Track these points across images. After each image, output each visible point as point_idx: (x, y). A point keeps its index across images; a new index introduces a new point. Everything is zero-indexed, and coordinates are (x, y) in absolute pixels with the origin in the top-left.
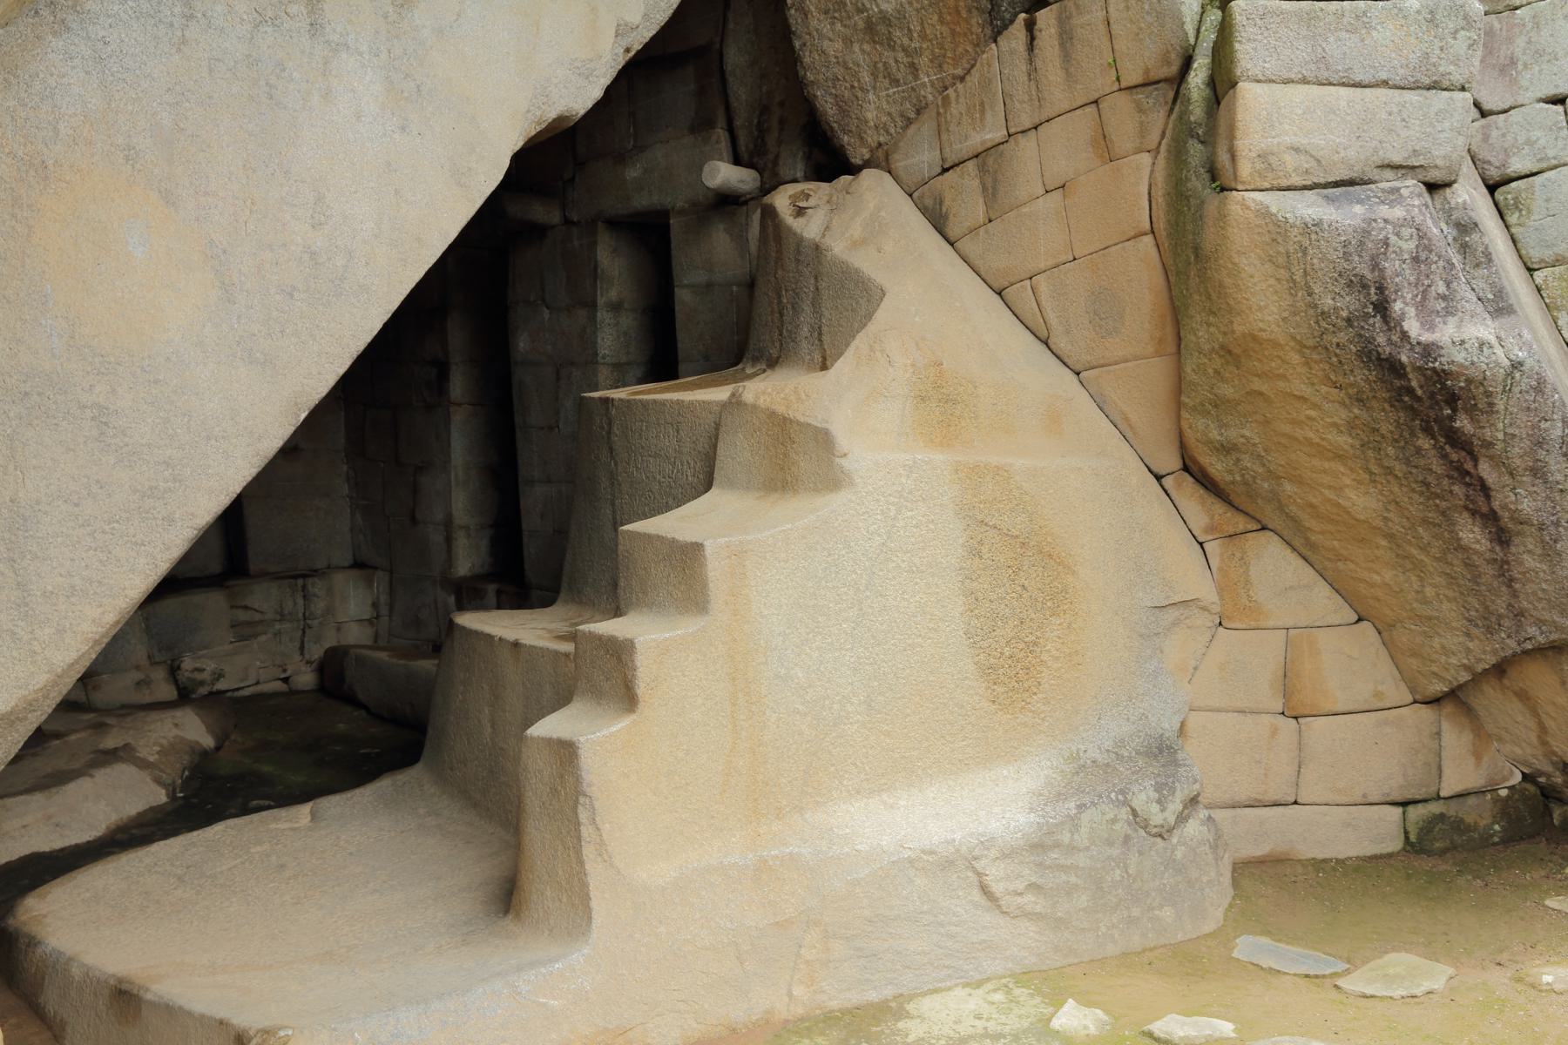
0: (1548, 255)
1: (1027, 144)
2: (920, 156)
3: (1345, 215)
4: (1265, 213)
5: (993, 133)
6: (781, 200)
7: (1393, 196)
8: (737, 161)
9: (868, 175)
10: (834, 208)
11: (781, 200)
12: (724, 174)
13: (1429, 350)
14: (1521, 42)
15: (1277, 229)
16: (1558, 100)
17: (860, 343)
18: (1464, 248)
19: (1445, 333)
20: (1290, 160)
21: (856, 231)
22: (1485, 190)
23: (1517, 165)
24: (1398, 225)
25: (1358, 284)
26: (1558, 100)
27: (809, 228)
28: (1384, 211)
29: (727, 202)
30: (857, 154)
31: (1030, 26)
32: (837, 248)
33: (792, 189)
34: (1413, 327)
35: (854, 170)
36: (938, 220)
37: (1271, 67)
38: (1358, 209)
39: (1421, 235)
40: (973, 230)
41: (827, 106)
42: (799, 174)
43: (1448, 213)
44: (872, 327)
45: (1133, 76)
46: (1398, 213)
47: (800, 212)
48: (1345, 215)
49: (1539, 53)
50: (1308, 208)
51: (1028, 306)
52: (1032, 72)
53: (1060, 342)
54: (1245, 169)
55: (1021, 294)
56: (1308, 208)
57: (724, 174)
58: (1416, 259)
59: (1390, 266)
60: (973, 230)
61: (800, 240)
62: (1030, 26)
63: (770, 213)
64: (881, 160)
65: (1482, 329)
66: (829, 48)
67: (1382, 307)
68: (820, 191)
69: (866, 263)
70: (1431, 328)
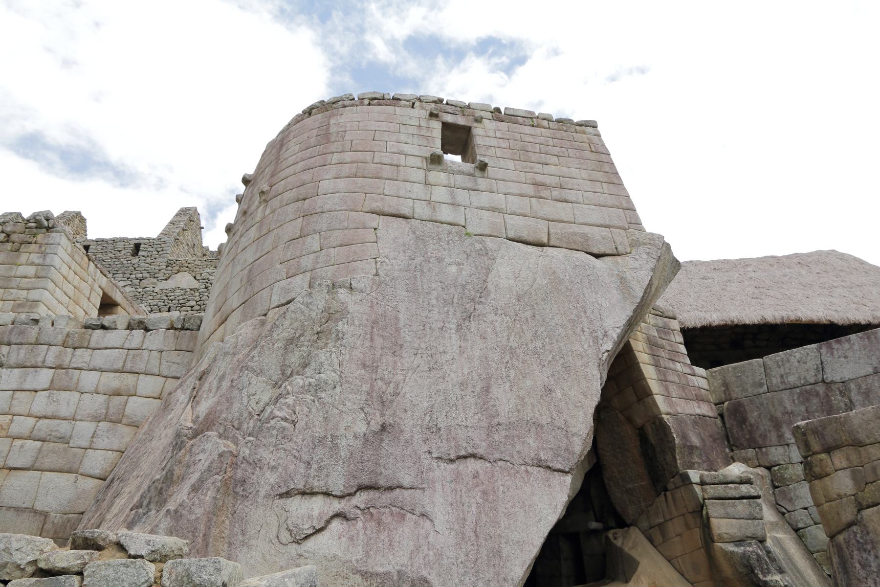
0: (815, 549)
1: (670, 524)
2: (645, 524)
3: (740, 550)
4: (721, 548)
5: (662, 520)
6: (610, 535)
7: (750, 545)
8: (597, 521)
9: (631, 528)
10: (624, 538)
11: (610, 535)
12: (594, 525)
13: (765, 582)
14: (792, 494)
15: (725, 553)
16: (806, 509)
17: (634, 577)
18: (769, 557)
19: (768, 578)
20: (725, 536)
21: (630, 544)
22: (793, 532)
23: (800, 525)
24: (752, 552)
25: (745, 566)
26: (806, 509)
27: (619, 543)
28: (749, 549)
29: (595, 532)
30: (629, 522)
31: (665, 495)
32: (626, 549)
33: (612, 531)
34: (761, 576)
35: (628, 526)
36: (651, 541)
37: (716, 515)
38: (742, 548)
39: (757, 554)
40: (660, 544)
41: (618, 508)
42: (614, 525)
43: (765, 547)
44: (637, 573)
45: (691, 510)
46: (751, 549)
47: (615, 538)
48: (740, 550)
49: (798, 497)
50: (731, 548)
51: (677, 565)
52: (667, 506)
53: (686, 576)
54: (716, 538)
55: (674, 561)
56: (731, 548)
57: (594, 525)
58: (758, 560)
59: (752, 562)
60: (660, 544)
61: (616, 547)
62: (665, 495)
63: (607, 538)
64: (634, 524)
65: (777, 577)
66: (617, 495)
67: (753, 571)
68: (620, 532)
69: (634, 554)
70: (765, 576)
